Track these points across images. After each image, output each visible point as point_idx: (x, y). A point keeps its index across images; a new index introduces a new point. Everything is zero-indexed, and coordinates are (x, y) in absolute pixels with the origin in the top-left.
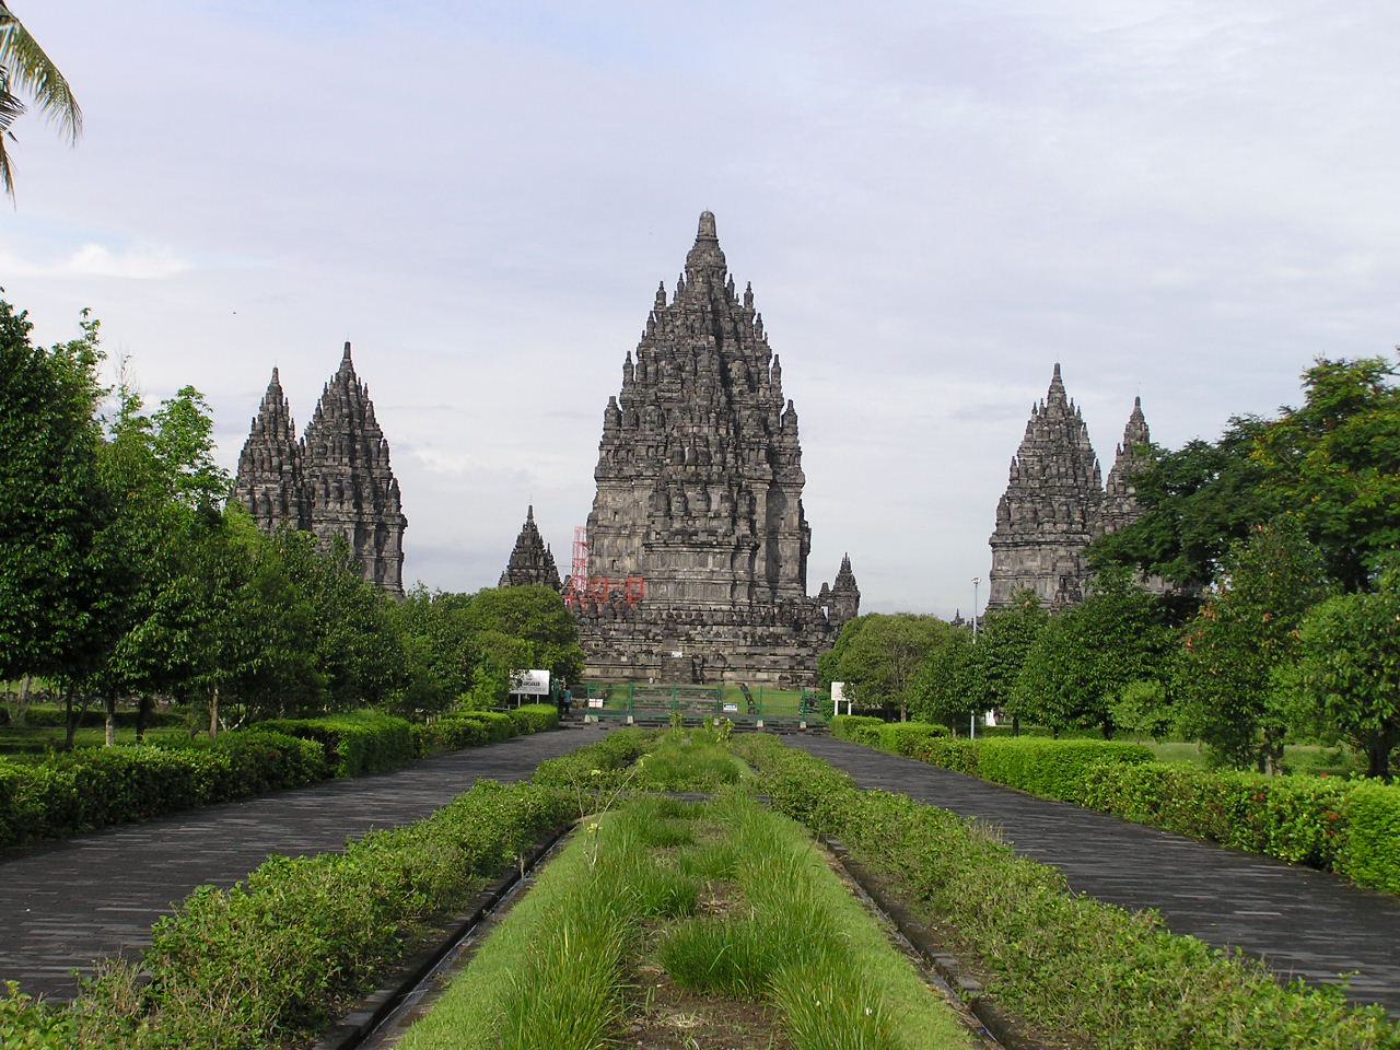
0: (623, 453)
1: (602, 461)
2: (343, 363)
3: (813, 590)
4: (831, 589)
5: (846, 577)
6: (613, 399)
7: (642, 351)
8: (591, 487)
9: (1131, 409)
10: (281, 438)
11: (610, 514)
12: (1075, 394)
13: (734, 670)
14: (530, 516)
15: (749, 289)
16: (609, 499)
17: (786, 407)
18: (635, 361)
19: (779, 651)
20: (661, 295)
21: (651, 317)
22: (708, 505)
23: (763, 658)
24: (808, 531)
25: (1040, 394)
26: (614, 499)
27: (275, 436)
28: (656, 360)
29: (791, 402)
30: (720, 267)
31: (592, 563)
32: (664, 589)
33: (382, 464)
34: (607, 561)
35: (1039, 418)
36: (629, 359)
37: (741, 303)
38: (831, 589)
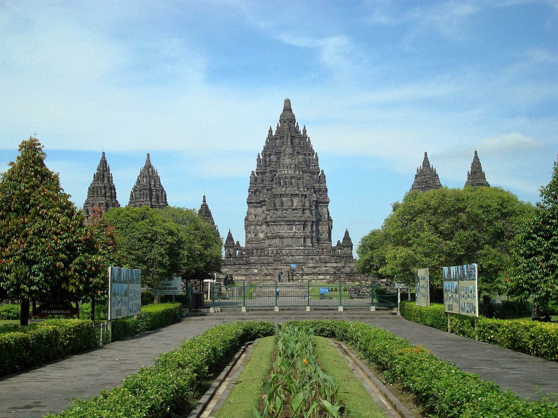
0: (257, 193)
1: (249, 196)
2: (147, 162)
3: (334, 244)
4: (341, 243)
5: (347, 237)
6: (253, 172)
7: (265, 153)
8: (246, 207)
9: (473, 155)
10: (106, 182)
11: (253, 217)
12: (433, 163)
13: (307, 275)
14: (204, 201)
15: (305, 128)
16: (253, 211)
17: (320, 173)
18: (261, 157)
19: (328, 265)
20: (271, 131)
21: (267, 140)
22: (292, 203)
23: (321, 269)
24: (331, 220)
25: (419, 164)
26: (255, 211)
27: (103, 181)
28: (270, 155)
29: (323, 171)
30: (292, 120)
31: (247, 236)
32: (274, 241)
33: (164, 200)
34: (253, 235)
35: (420, 173)
36: (259, 156)
37: (302, 133)
38: (341, 243)
